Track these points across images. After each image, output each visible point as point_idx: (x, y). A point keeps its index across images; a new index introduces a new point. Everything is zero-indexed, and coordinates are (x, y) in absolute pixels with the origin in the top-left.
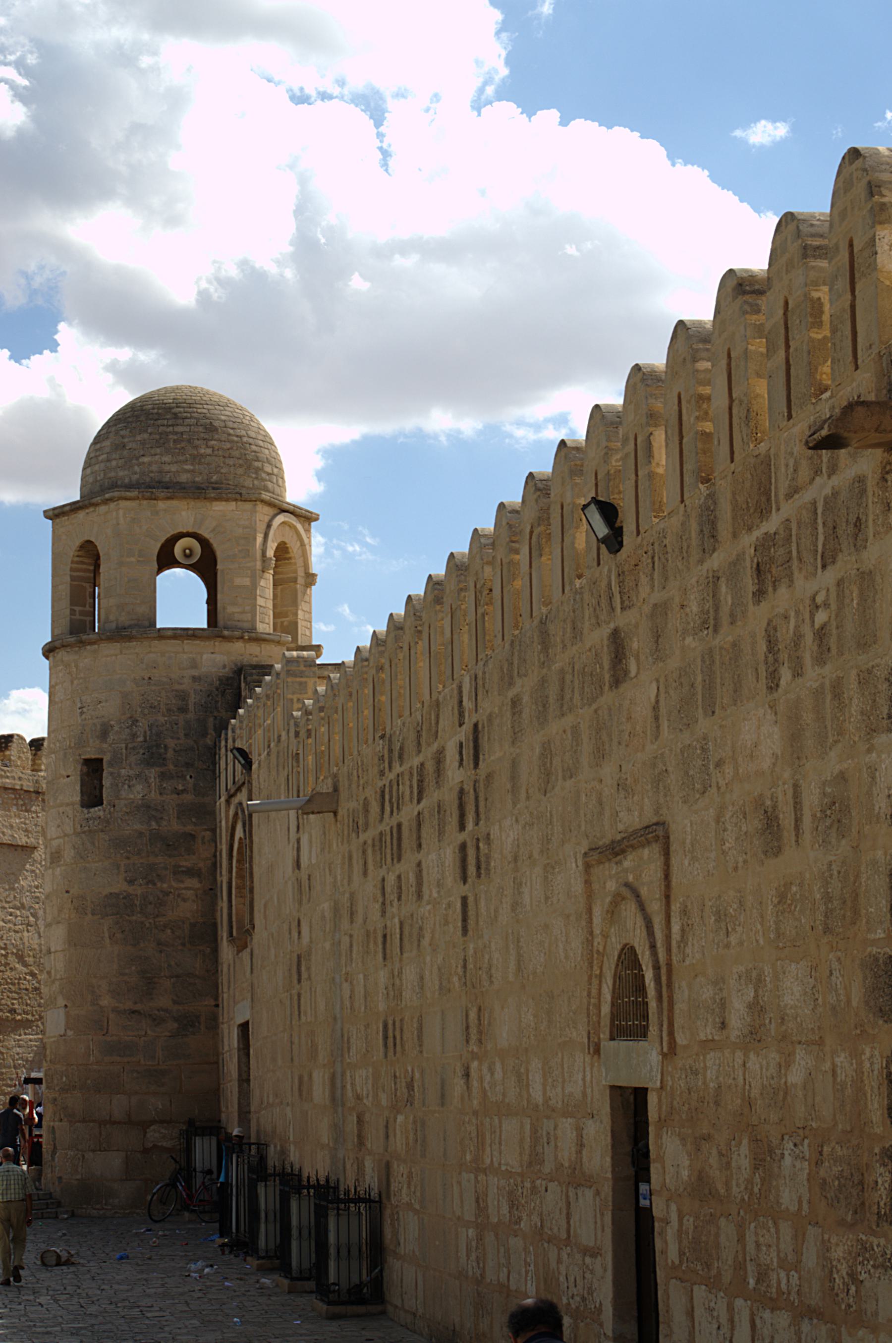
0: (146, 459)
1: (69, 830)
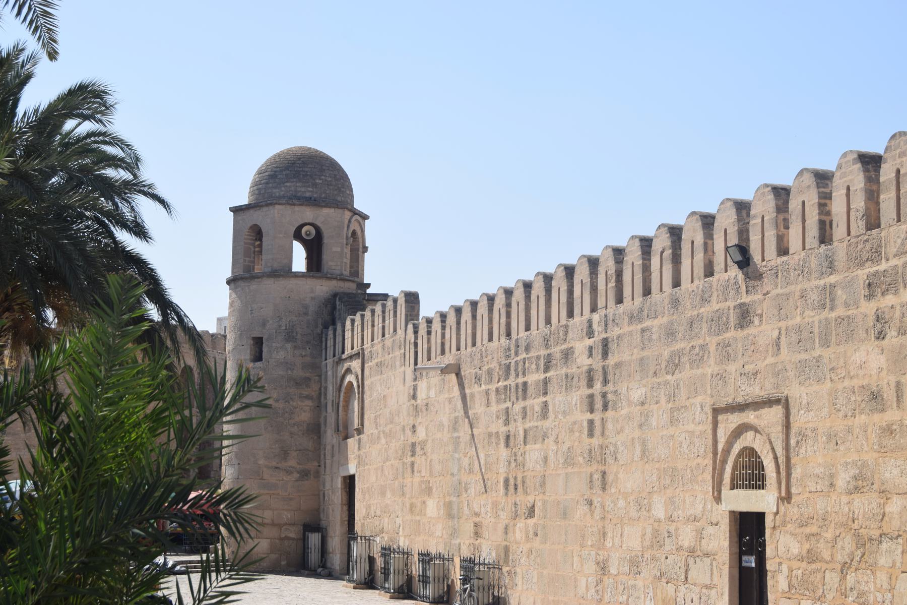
0: (288, 184)
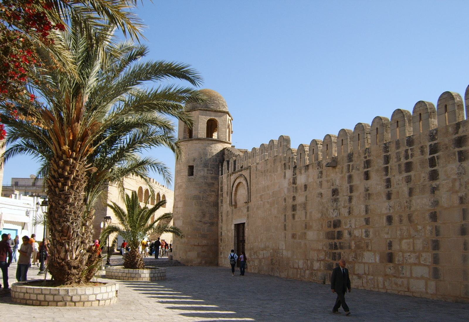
1: (184, 181)
